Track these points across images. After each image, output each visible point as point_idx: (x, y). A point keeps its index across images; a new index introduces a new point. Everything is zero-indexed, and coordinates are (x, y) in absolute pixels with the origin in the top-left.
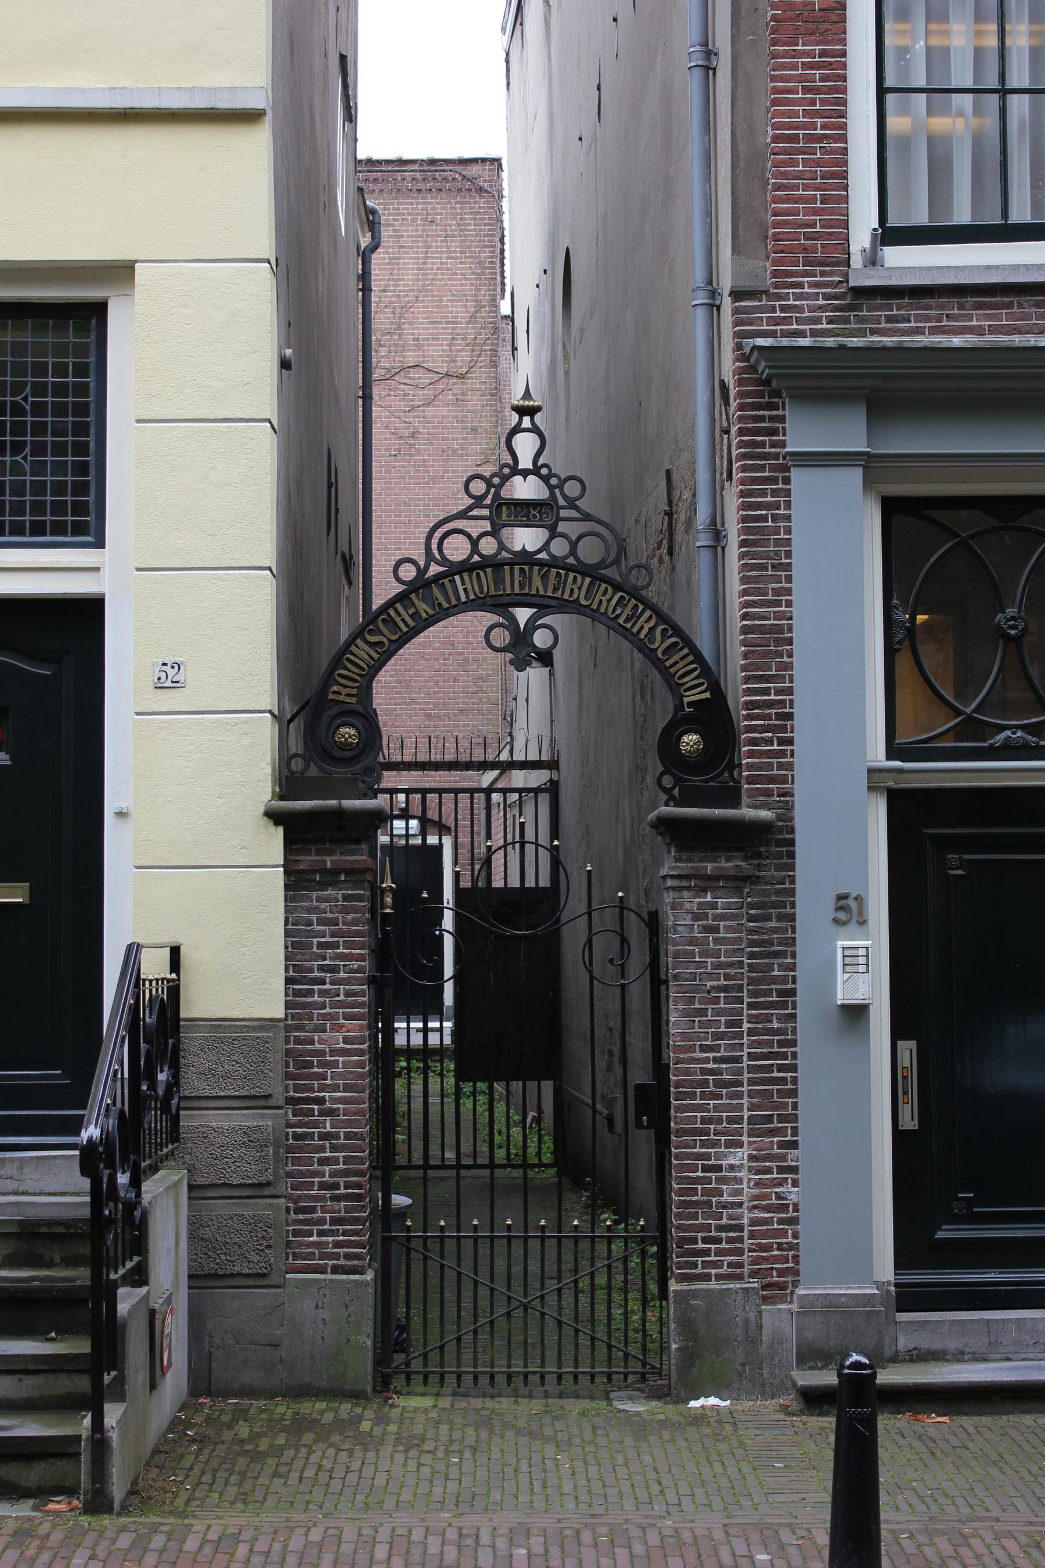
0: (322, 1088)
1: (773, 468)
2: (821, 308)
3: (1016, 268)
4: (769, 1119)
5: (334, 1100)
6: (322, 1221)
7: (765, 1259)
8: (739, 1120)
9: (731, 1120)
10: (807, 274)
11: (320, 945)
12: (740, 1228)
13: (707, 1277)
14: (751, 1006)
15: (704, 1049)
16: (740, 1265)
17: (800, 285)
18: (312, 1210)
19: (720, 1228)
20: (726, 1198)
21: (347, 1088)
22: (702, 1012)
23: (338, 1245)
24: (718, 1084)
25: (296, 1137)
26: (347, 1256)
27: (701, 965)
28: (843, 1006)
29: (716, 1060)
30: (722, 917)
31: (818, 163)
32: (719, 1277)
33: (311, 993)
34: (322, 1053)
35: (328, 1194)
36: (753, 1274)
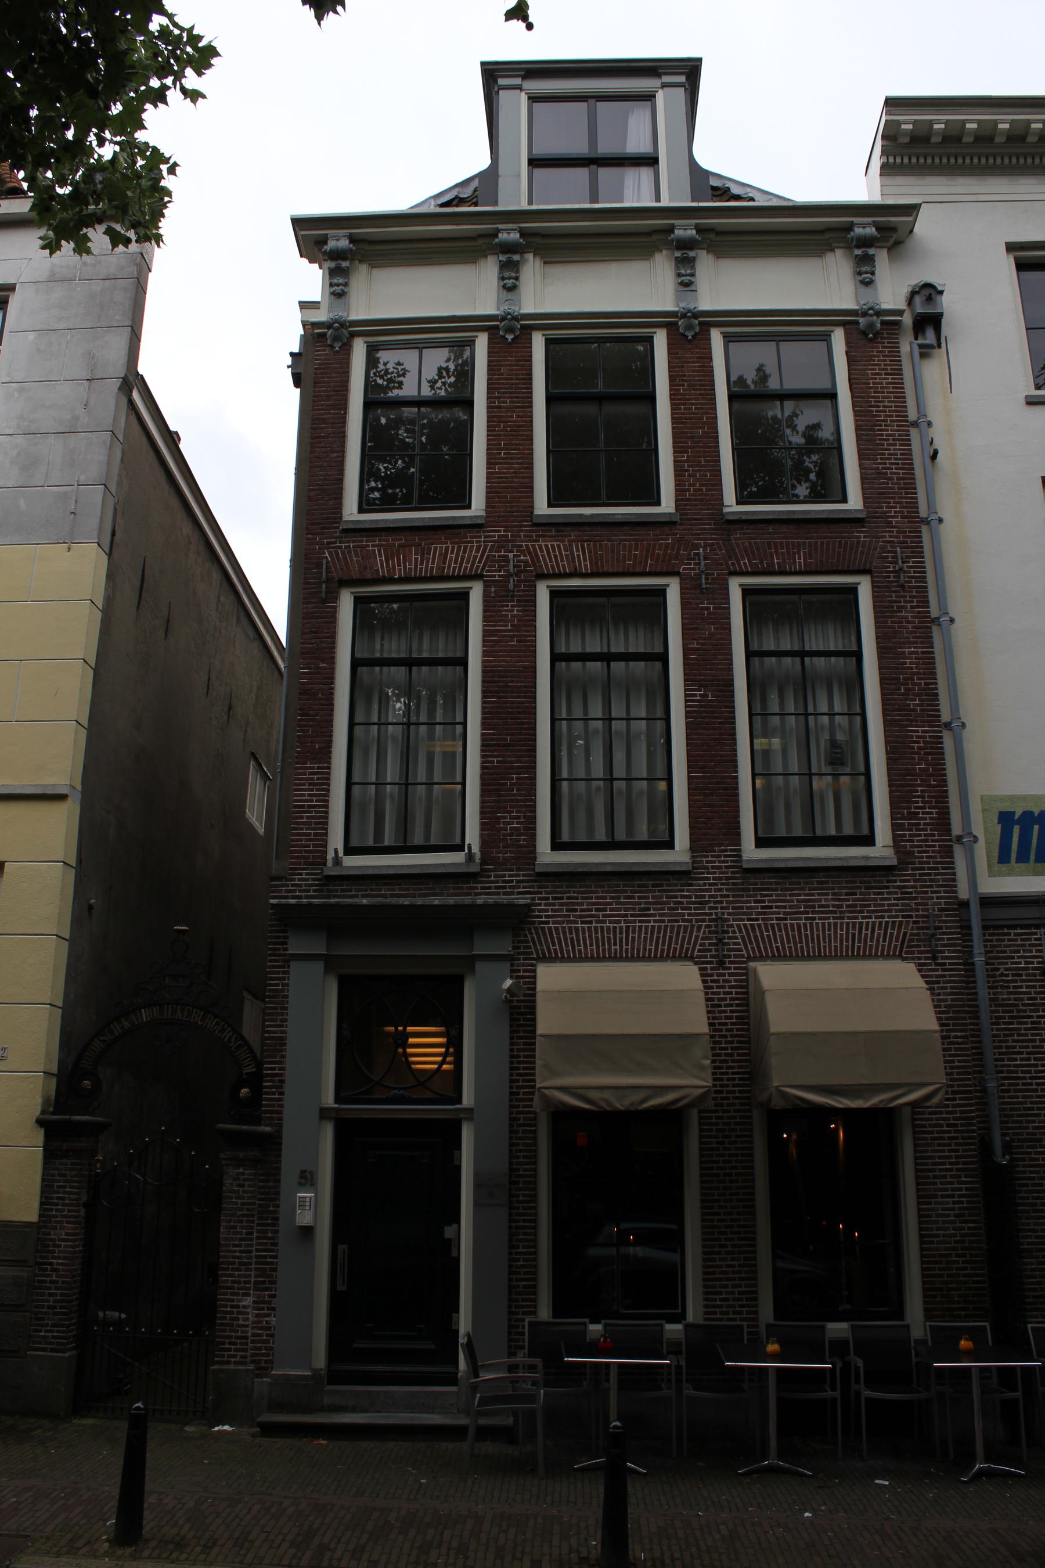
0: (54, 1258)
1: (283, 961)
2: (311, 885)
3: (402, 866)
4: (264, 1282)
5: (59, 1264)
6: (47, 1325)
7: (258, 1355)
8: (249, 1282)
9: (246, 1282)
10: (304, 869)
11: (58, 1187)
12: (246, 1338)
13: (229, 1363)
14: (258, 1225)
15: (235, 1246)
16: (245, 1357)
17: (301, 874)
18: (43, 1319)
19: (237, 1338)
20: (241, 1322)
21: (65, 1258)
22: (235, 1227)
23: (53, 1337)
24: (240, 1264)
25: (39, 1282)
26: (58, 1343)
27: (235, 1203)
28: (301, 1227)
29: (240, 1252)
30: (245, 1180)
31: (313, 818)
32: (236, 1363)
33: (52, 1210)
34: (54, 1240)
35: (51, 1311)
36: (252, 1362)
